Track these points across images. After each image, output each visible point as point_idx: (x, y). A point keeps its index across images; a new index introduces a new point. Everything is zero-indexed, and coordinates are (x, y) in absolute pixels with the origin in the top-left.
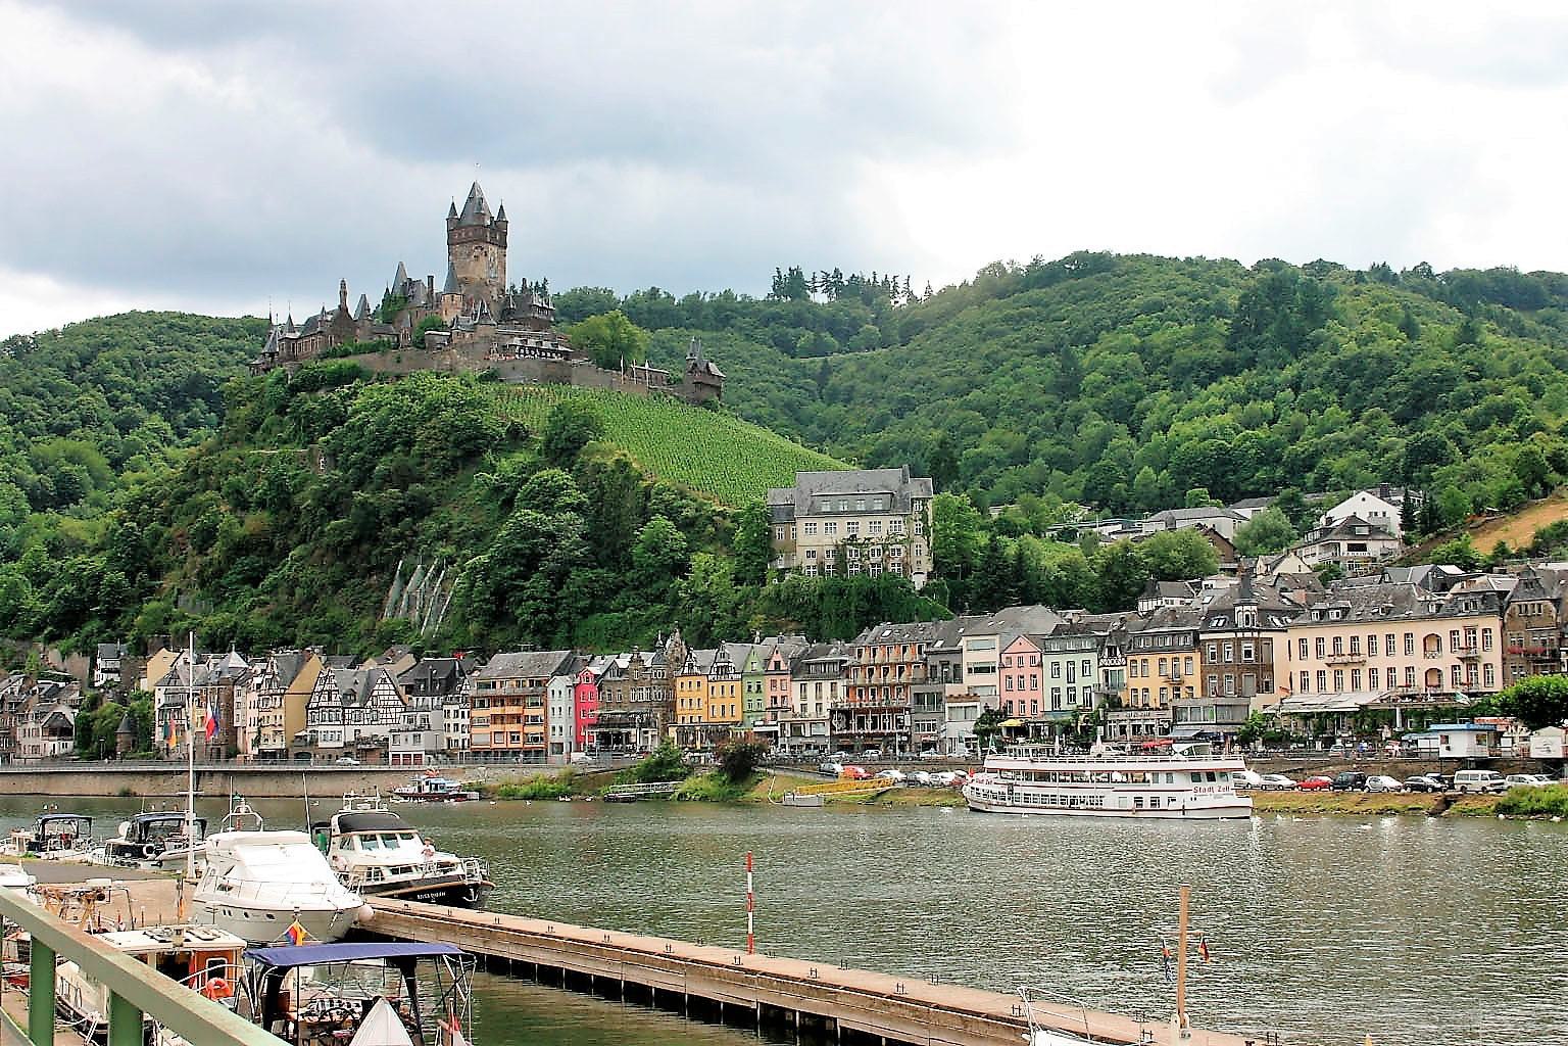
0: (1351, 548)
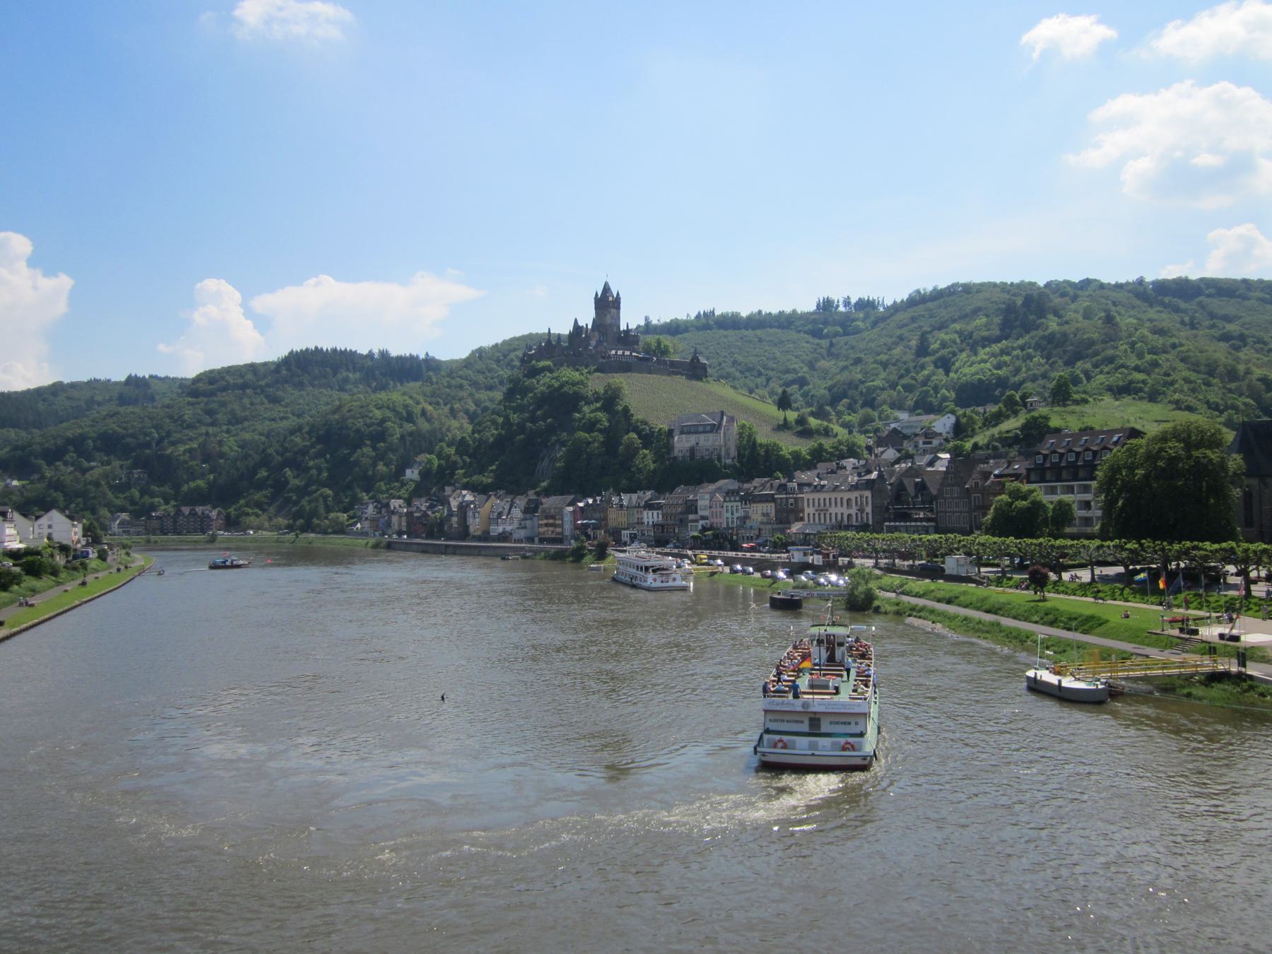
0: (924, 443)
